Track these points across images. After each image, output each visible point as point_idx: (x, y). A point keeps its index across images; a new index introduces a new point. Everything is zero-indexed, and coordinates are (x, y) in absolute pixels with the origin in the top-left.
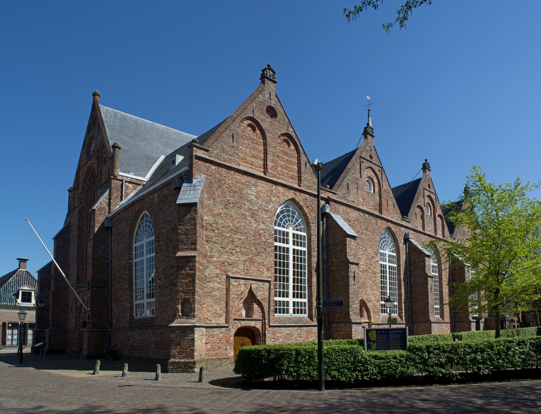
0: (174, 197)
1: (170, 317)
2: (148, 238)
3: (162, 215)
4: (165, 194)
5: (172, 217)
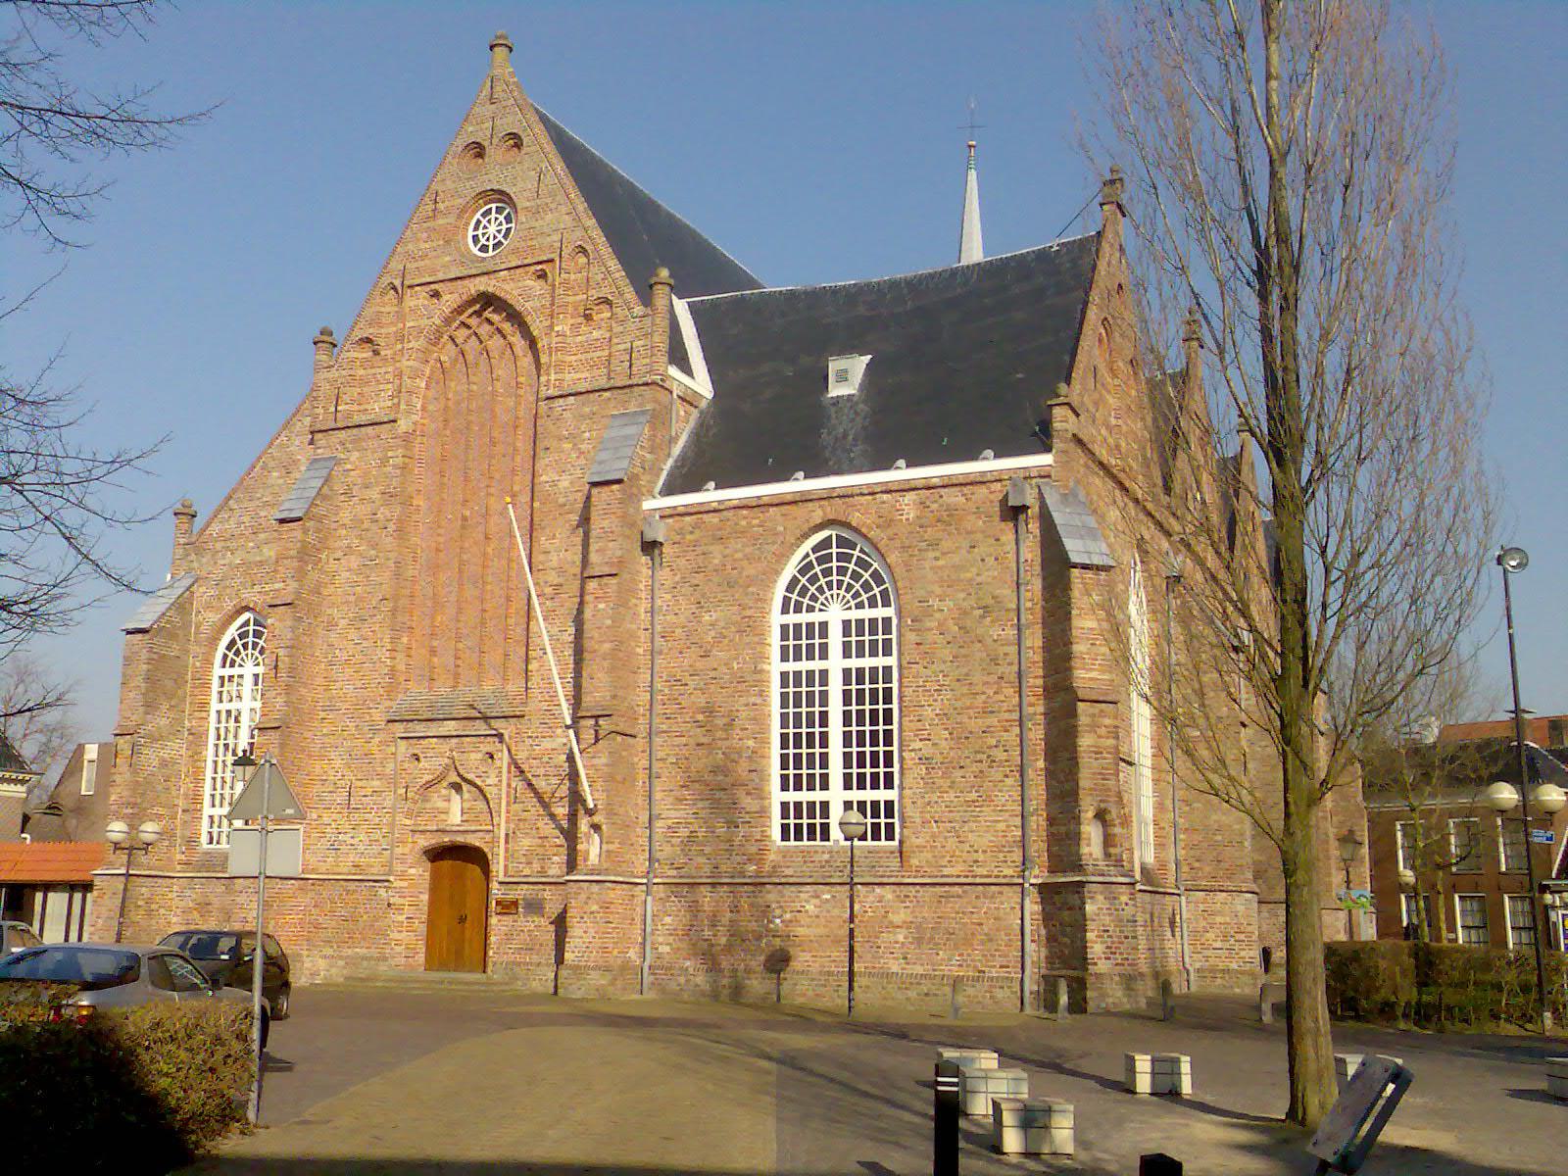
0: (984, 522)
1: (976, 851)
2: (850, 608)
3: (937, 559)
4: (948, 505)
5: (978, 575)
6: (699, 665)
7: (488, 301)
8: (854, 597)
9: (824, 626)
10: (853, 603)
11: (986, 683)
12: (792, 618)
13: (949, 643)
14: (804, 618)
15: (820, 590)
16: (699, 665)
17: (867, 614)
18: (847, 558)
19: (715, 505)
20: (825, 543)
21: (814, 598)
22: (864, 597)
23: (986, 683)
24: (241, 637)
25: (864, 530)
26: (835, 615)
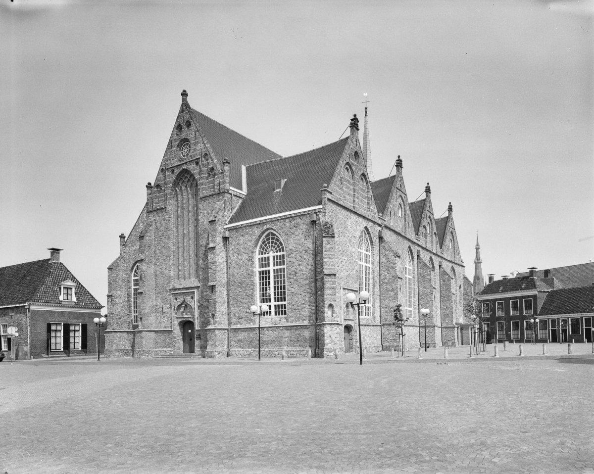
6: (239, 271)
9: (268, 258)
10: (275, 251)
11: (306, 271)
14: (264, 256)
15: (267, 248)
16: (239, 271)
17: (279, 254)
20: (268, 235)
21: (266, 250)
22: (278, 249)
23: (306, 271)
26: (271, 255)
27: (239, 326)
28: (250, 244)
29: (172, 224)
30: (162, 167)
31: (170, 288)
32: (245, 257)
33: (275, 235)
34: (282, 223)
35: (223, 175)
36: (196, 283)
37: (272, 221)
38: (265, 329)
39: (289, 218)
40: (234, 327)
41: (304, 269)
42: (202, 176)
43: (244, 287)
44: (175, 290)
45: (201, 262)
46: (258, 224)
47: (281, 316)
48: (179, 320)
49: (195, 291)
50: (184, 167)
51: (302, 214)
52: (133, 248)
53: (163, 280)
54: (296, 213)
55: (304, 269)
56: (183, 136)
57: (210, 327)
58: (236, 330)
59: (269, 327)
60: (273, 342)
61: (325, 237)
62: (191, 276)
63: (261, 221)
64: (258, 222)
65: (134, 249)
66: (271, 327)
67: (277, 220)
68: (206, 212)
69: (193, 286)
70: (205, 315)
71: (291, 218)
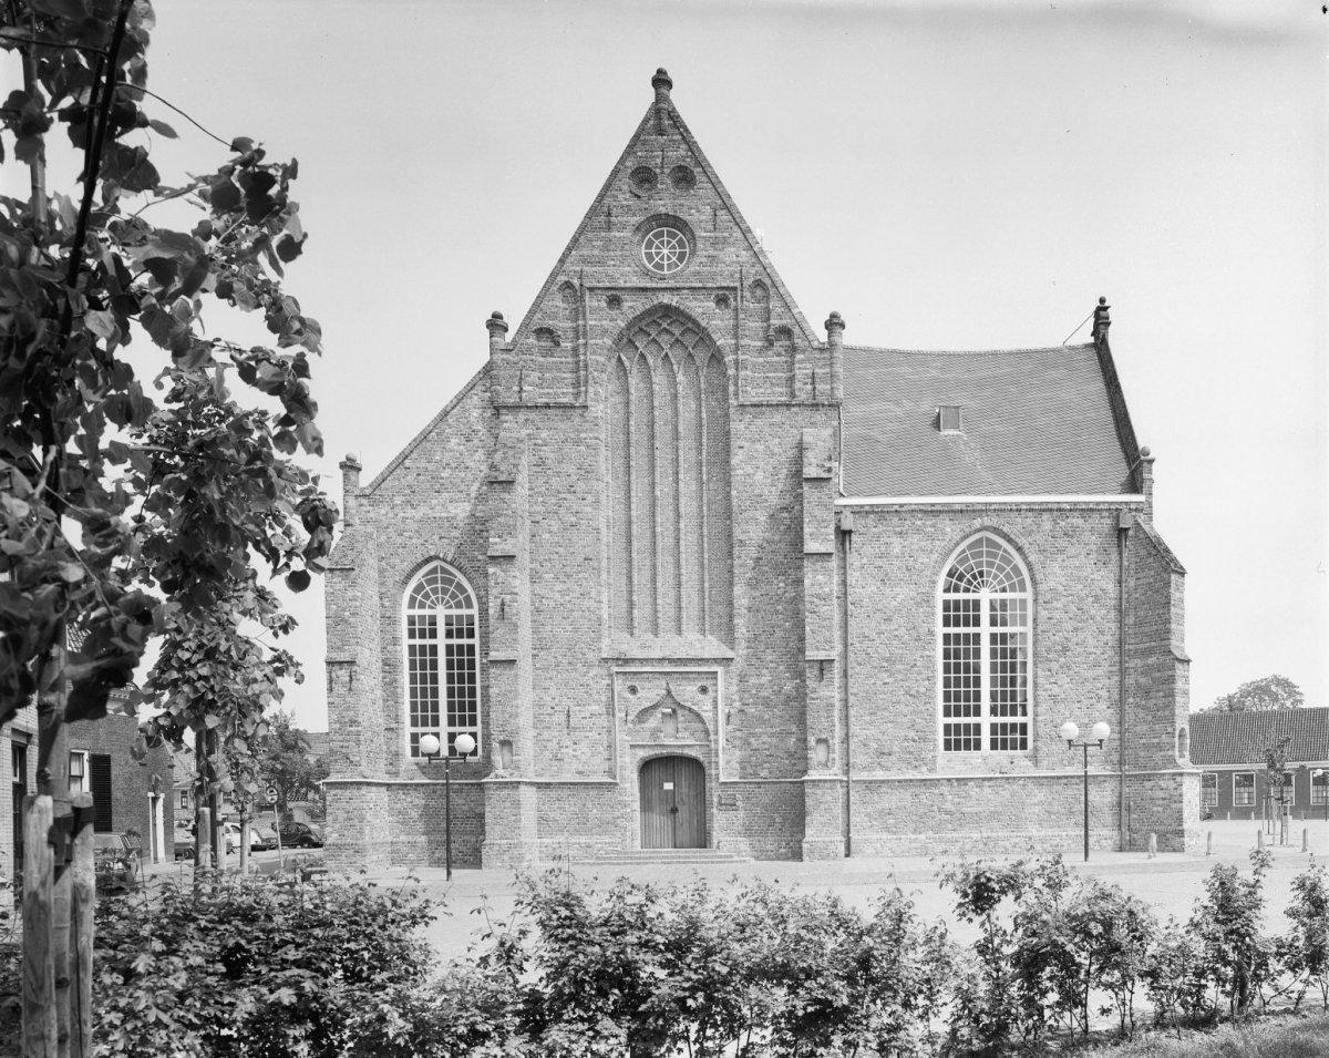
2: (996, 591)
6: (884, 627)
7: (667, 311)
8: (999, 583)
9: (977, 604)
12: (952, 596)
13: (1071, 618)
18: (995, 556)
19: (896, 507)
24: (429, 582)
25: (1012, 536)
26: (985, 596)
27: (880, 775)
28: (926, 560)
29: (606, 464)
30: (562, 278)
31: (605, 656)
32: (904, 592)
33: (999, 547)
34: (1029, 521)
35: (827, 355)
36: (713, 647)
37: (1001, 510)
38: (970, 784)
39: (1051, 510)
40: (864, 776)
41: (1091, 641)
42: (742, 342)
43: (899, 672)
44: (627, 661)
45: (738, 590)
46: (955, 512)
47: (1009, 752)
48: (643, 754)
49: (720, 670)
50: (666, 299)
51: (1091, 506)
52: (410, 512)
53: (570, 628)
54: (1075, 504)
55: (1091, 641)
56: (663, 204)
57: (813, 775)
58: (870, 785)
59: (984, 779)
60: (994, 816)
61: (1174, 571)
62: (684, 627)
63: (967, 505)
64: (957, 507)
65: (418, 514)
66: (990, 779)
67: (1018, 509)
68: (760, 447)
69: (706, 656)
70: (752, 740)
71: (1059, 510)
